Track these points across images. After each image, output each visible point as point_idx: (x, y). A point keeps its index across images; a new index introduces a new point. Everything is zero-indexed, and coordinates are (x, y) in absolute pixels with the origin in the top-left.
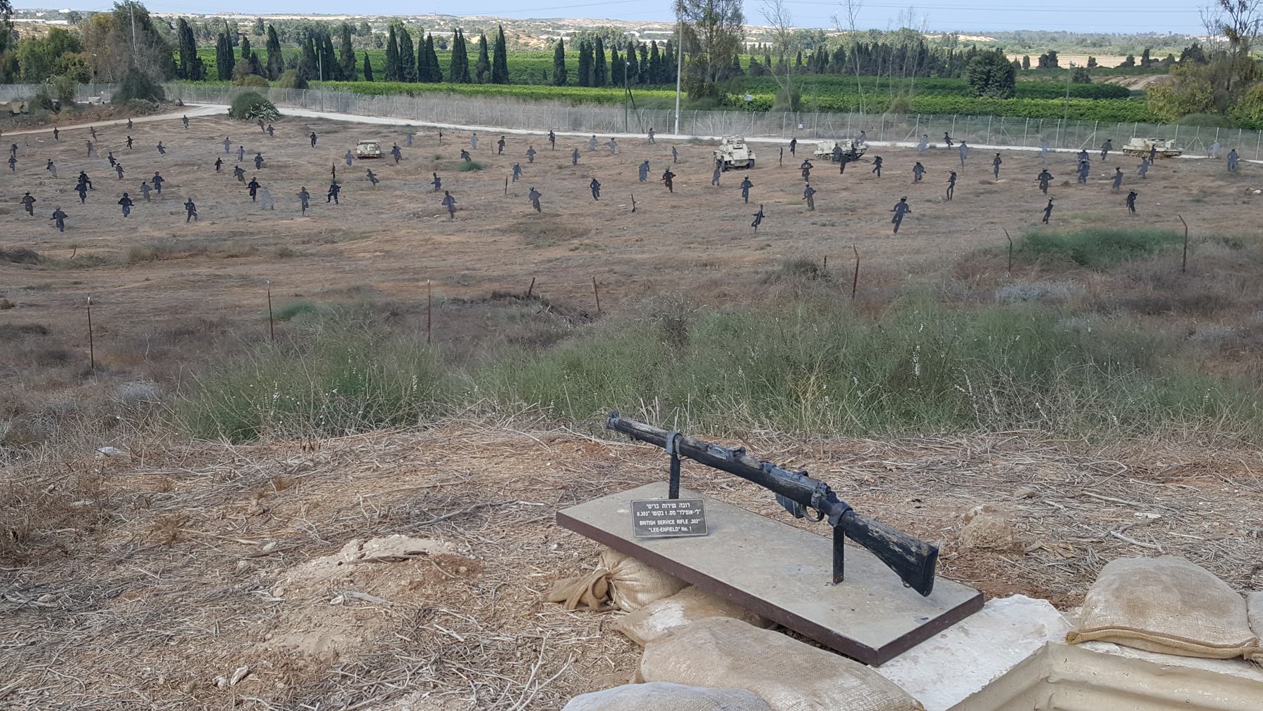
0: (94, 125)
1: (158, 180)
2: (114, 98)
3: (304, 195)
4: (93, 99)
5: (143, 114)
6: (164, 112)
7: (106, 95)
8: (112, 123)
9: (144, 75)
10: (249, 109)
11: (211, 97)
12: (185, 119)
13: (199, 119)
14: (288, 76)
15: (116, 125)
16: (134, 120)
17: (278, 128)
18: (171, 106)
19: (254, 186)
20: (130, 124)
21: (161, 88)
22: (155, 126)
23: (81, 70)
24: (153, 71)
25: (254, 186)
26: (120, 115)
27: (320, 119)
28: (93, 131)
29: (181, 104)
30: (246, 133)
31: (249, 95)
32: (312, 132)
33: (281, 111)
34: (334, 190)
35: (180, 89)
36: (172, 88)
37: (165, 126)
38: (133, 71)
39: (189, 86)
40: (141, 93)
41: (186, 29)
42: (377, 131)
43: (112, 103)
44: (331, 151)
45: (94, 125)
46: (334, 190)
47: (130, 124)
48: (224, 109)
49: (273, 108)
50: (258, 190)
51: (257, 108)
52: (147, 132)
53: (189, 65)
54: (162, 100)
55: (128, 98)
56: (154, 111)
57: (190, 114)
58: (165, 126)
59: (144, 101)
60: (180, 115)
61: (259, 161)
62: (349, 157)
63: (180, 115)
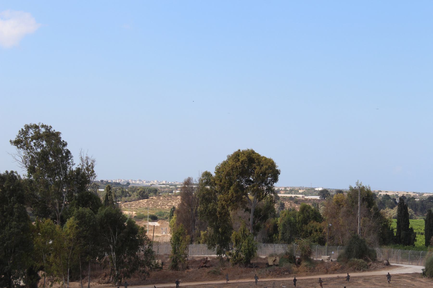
0: (323, 276)
2: (340, 257)
4: (325, 258)
6: (375, 269)
7: (335, 254)
9: (363, 241)
11: (413, 260)
12: (389, 276)
13: (400, 276)
15: (338, 278)
16: (352, 275)
18: (380, 265)
21: (374, 251)
23: (321, 235)
24: (371, 239)
26: (342, 270)
28: (320, 281)
29: (388, 264)
35: (389, 253)
36: (382, 252)
37: (373, 281)
38: (356, 238)
39: (397, 251)
40: (359, 255)
41: (404, 205)
43: (338, 261)
45: (323, 276)
47: (348, 278)
52: (360, 284)
53: (403, 233)
54: (375, 260)
55: (349, 257)
56: (367, 268)
57: (393, 272)
58: (373, 281)
59: (361, 260)
60: (385, 272)
63: (385, 272)
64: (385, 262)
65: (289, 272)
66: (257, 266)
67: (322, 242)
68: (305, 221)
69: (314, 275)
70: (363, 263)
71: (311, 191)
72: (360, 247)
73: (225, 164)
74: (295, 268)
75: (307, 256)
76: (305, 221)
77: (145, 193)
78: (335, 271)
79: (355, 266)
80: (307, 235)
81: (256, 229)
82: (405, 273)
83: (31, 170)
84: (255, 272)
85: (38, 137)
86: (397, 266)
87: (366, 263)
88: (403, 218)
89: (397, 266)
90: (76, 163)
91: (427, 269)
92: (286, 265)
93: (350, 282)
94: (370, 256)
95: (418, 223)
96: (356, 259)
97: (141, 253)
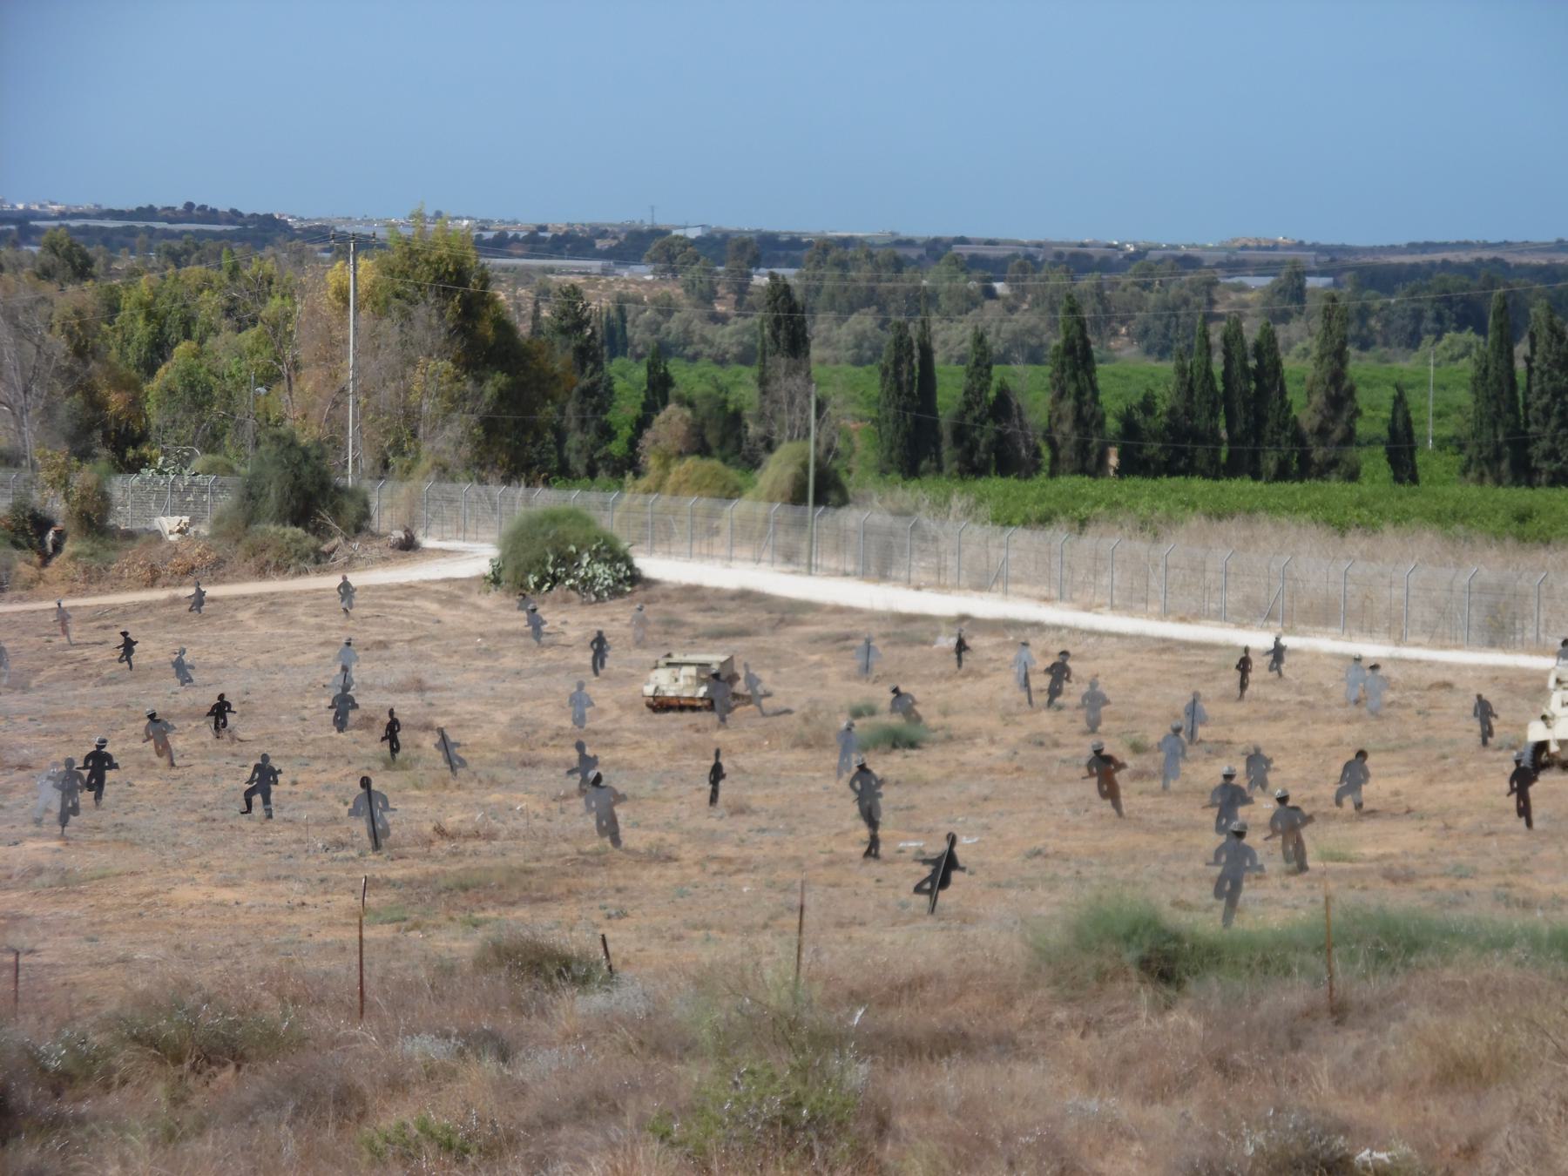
5: (281, 569)
8: (160, 594)
20: (199, 600)
27: (745, 597)
29: (408, 545)
31: (554, 519)
33: (650, 565)
47: (199, 600)
48: (476, 556)
49: (614, 555)
50: (110, 775)
51: (567, 560)
54: (360, 526)
55: (250, 520)
56: (320, 560)
64: (399, 534)
69: (101, 592)
70: (298, 541)
72: (297, 477)
75: (93, 519)
79: (268, 555)
82: (439, 576)
86: (445, 553)
87: (312, 541)
89: (445, 553)
91: (503, 558)
93: (203, 618)
94: (336, 512)
96: (272, 528)
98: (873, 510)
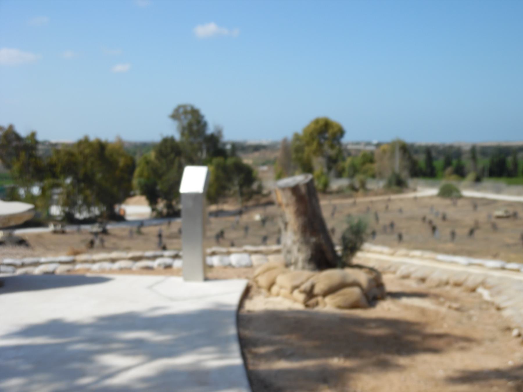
1: (392, 225)
3: (453, 234)
10: (447, 192)
11: (432, 186)
13: (423, 198)
14: (471, 176)
17: (460, 202)
19: (434, 229)
22: (401, 200)
25: (434, 229)
28: (372, 202)
30: (444, 205)
32: (475, 203)
34: (471, 232)
36: (411, 182)
42: (511, 204)
44: (482, 215)
46: (471, 232)
61: (444, 218)
62: (489, 216)
65: (350, 196)
66: (331, 193)
67: (373, 176)
68: (364, 163)
71: (368, 144)
73: (308, 127)
74: (354, 193)
75: (363, 185)
76: (364, 163)
77: (257, 148)
78: (381, 194)
80: (365, 172)
81: (329, 168)
83: (183, 134)
84: (329, 197)
85: (186, 113)
88: (430, 159)
90: (210, 130)
92: (349, 192)
95: (438, 163)
97: (255, 186)
98: (488, 182)
